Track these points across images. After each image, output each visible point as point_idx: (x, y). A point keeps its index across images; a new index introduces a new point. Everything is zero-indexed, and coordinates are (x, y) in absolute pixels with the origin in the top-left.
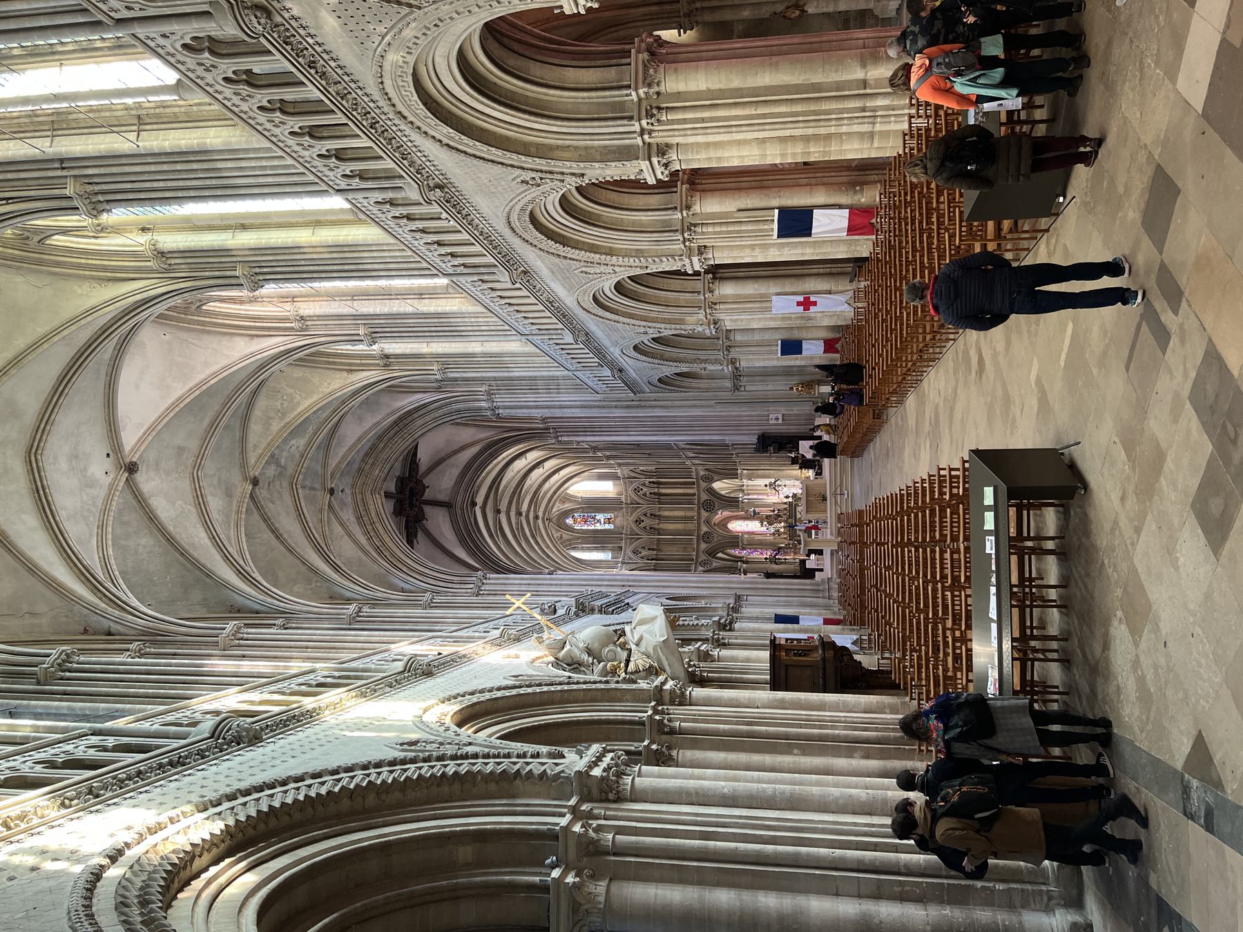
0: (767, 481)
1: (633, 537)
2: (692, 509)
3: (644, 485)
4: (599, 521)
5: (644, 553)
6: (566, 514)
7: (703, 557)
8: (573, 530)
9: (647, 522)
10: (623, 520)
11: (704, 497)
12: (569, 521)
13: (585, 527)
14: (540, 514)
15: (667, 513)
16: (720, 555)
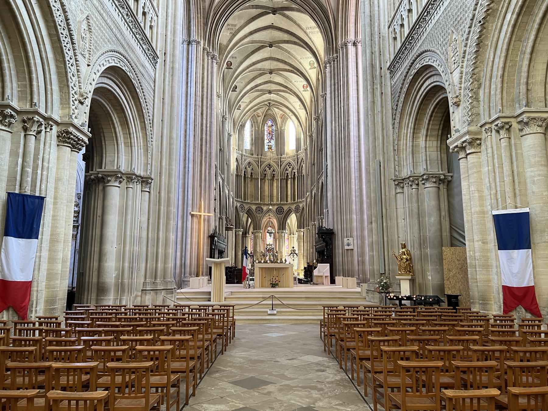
0: (296, 248)
1: (260, 162)
2: (277, 200)
3: (293, 169)
4: (270, 142)
5: (249, 170)
6: (274, 120)
7: (246, 207)
8: (263, 125)
9: (269, 172)
10: (270, 155)
11: (286, 208)
12: (270, 123)
13: (266, 133)
14: (273, 96)
15: (275, 185)
16: (250, 220)
